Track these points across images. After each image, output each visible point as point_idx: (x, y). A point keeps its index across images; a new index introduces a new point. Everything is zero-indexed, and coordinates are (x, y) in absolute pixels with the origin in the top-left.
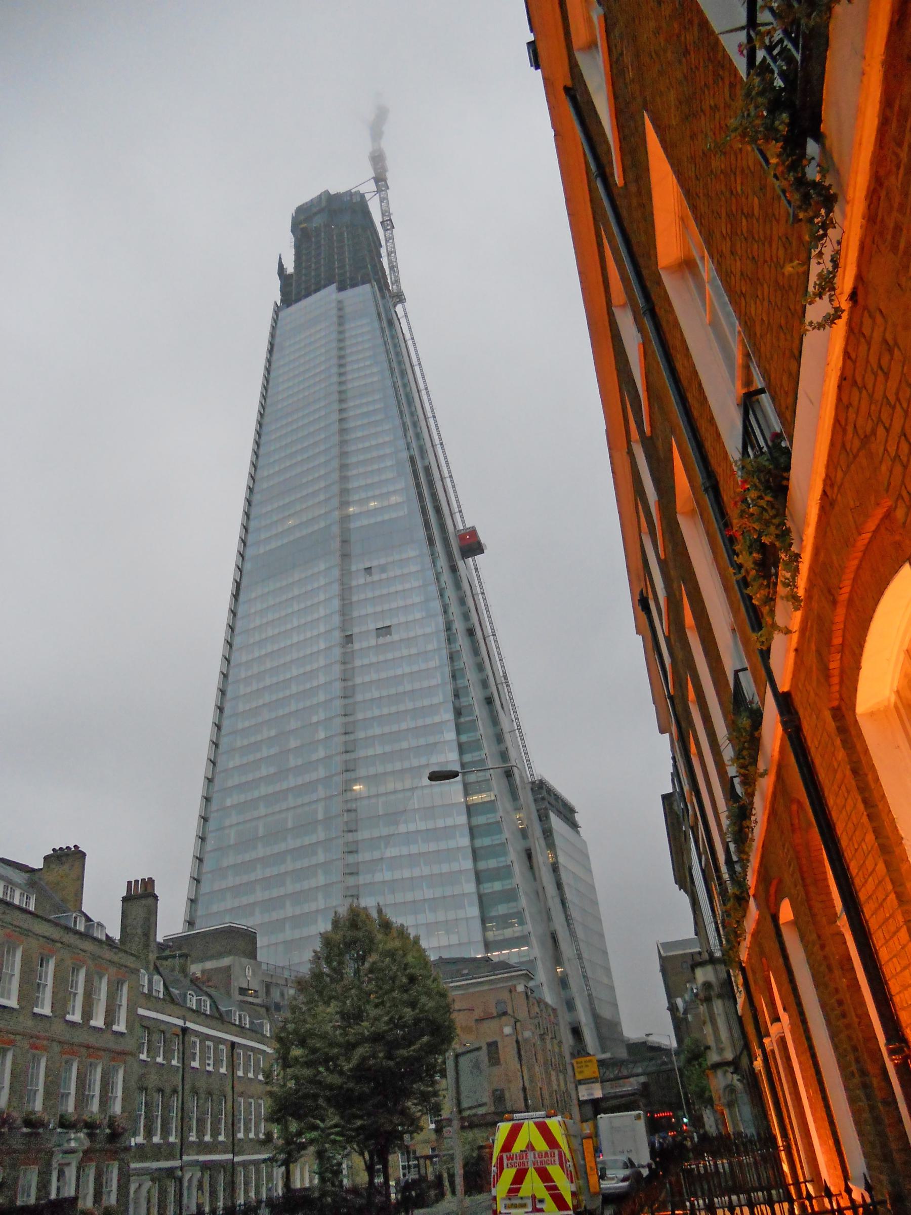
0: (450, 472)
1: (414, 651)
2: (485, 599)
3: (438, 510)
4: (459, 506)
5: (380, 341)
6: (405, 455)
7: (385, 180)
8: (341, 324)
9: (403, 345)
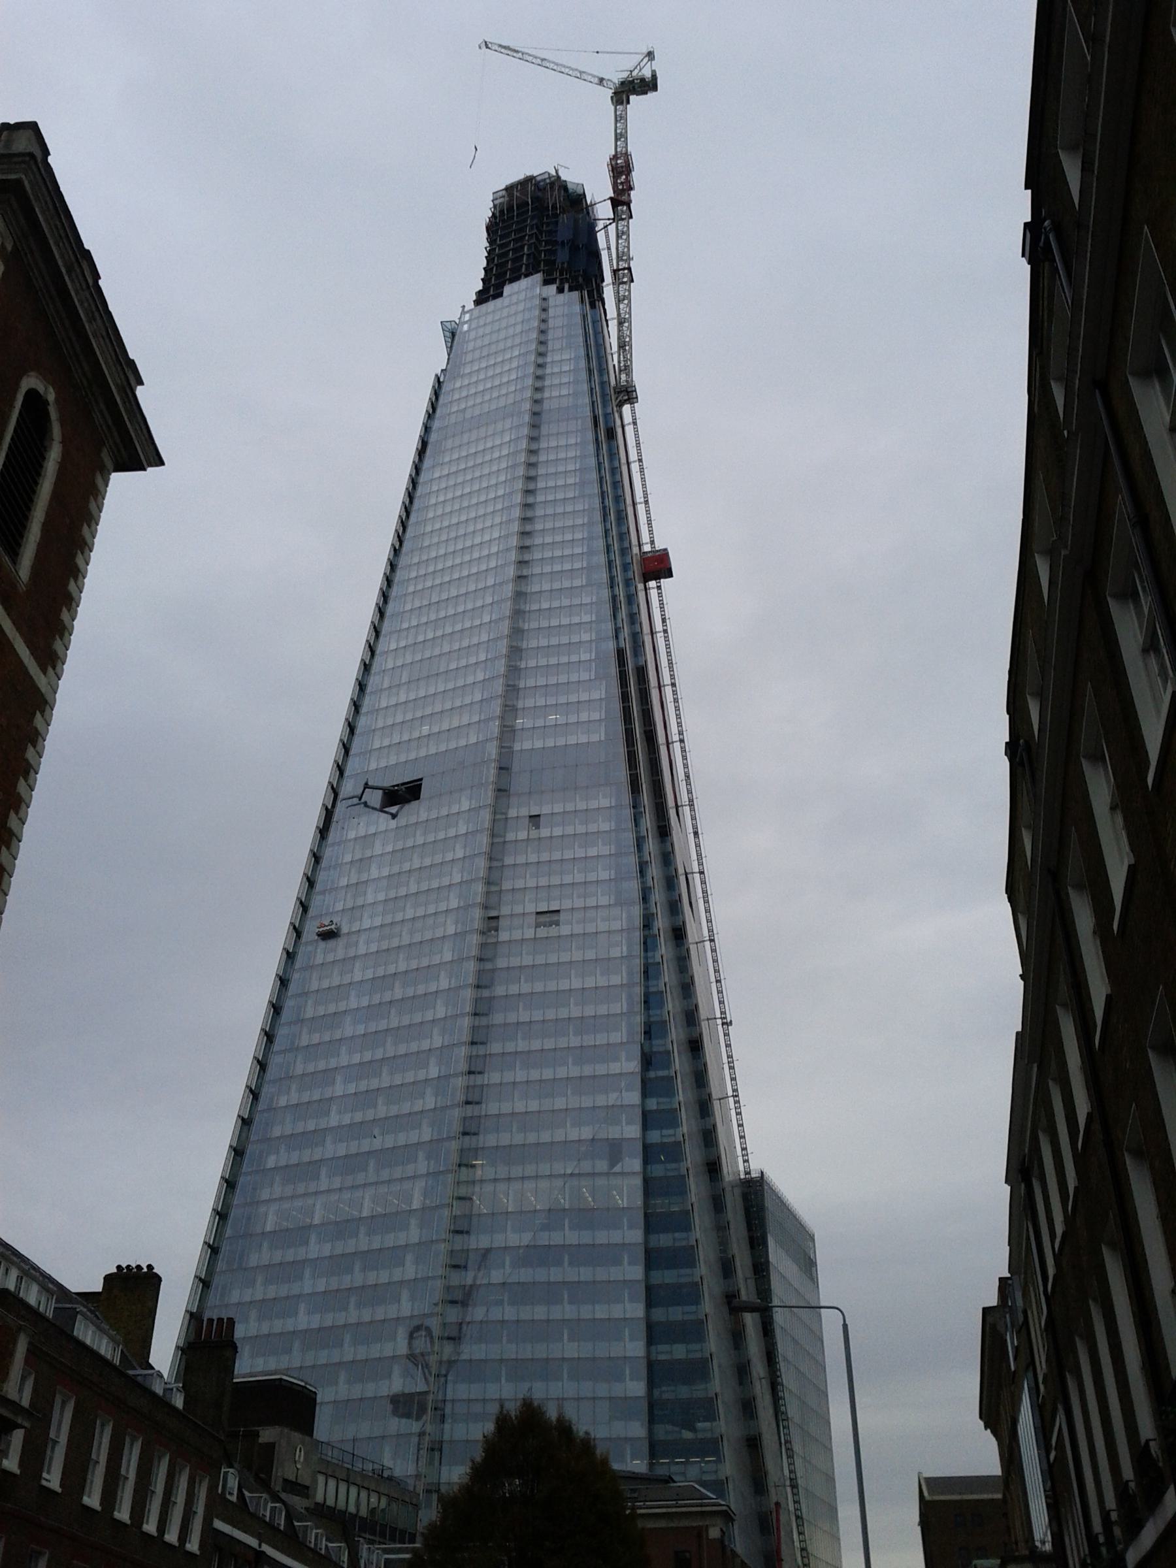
0: (672, 677)
1: (590, 955)
2: (703, 882)
4: (681, 733)
5: (592, 462)
6: (611, 646)
7: (628, 204)
8: (535, 426)
9: (624, 469)
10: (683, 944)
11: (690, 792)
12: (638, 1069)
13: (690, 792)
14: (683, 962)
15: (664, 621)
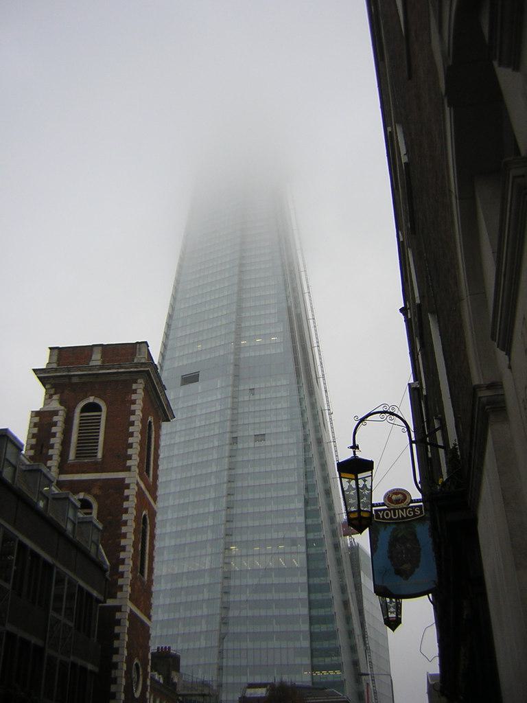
0: (313, 315)
1: (280, 455)
10: (321, 446)
11: (323, 371)
12: (303, 507)
13: (323, 371)
15: (308, 287)
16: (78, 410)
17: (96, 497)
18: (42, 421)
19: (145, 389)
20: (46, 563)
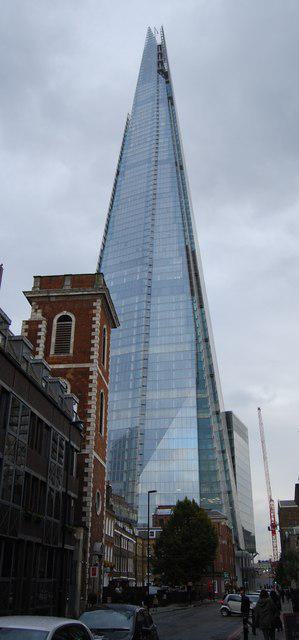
3: (197, 275)
6: (183, 245)
14: (208, 348)
16: (55, 321)
17: (69, 380)
18: (31, 326)
19: (102, 306)
20: (47, 426)
